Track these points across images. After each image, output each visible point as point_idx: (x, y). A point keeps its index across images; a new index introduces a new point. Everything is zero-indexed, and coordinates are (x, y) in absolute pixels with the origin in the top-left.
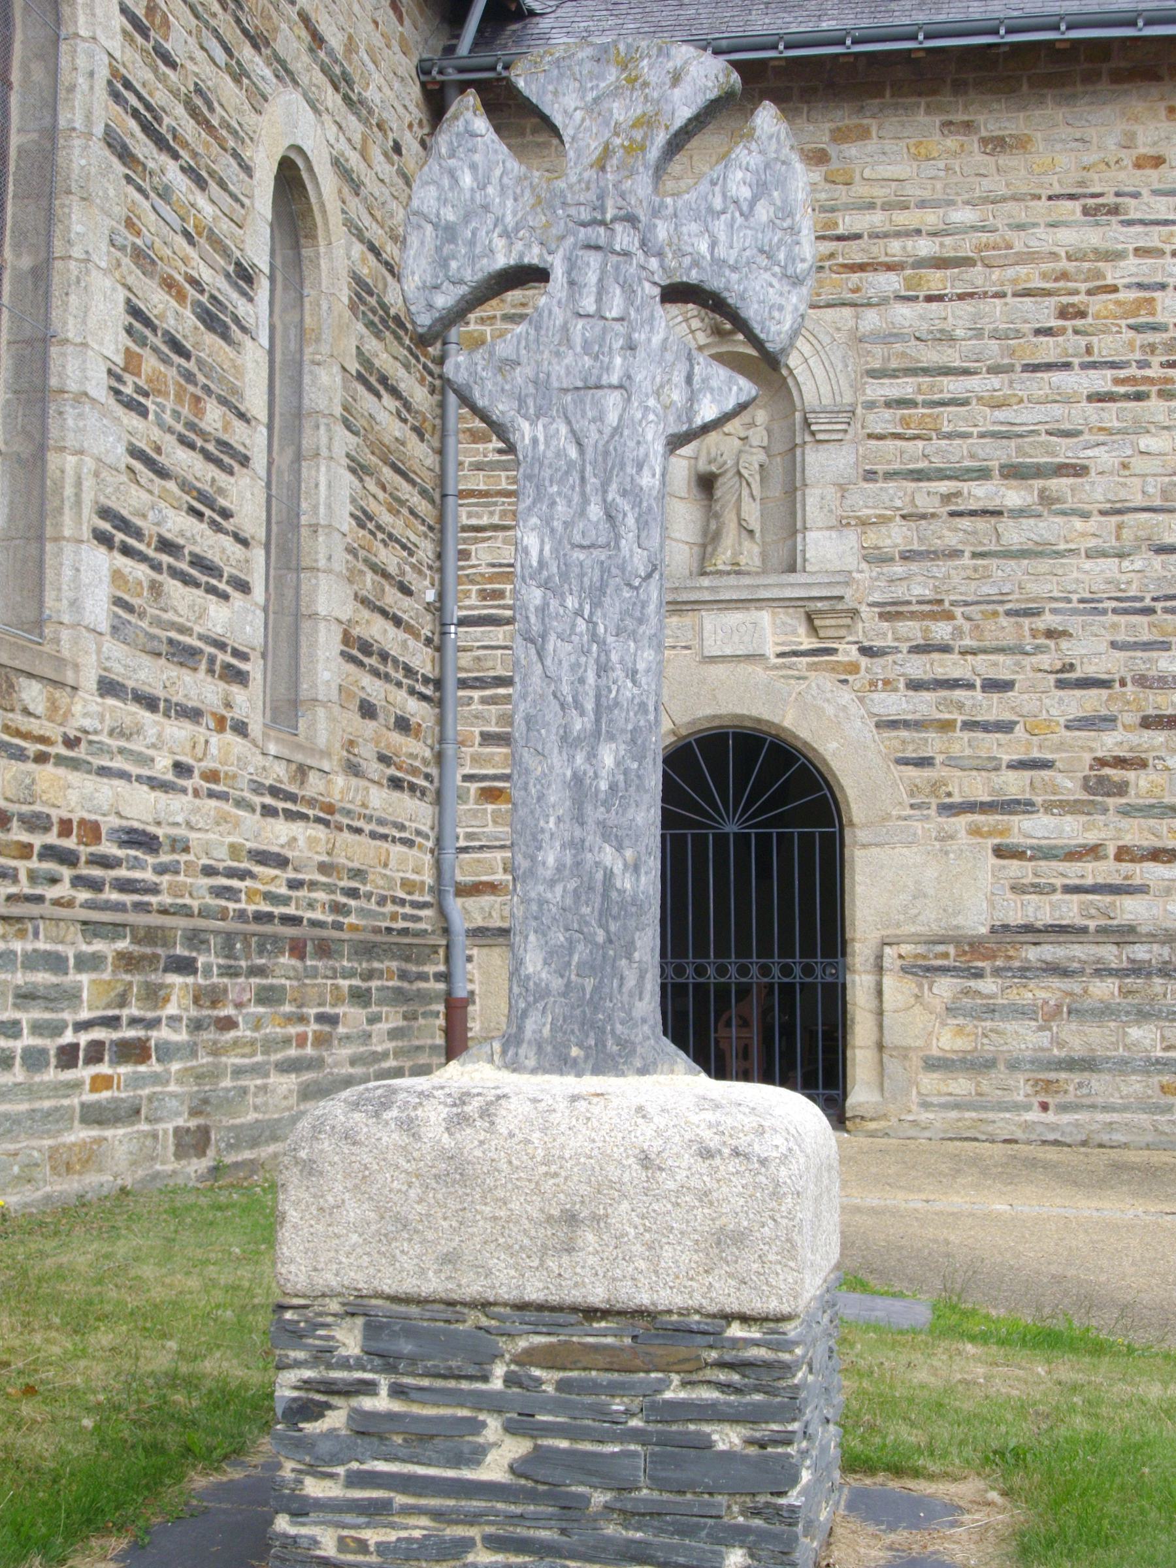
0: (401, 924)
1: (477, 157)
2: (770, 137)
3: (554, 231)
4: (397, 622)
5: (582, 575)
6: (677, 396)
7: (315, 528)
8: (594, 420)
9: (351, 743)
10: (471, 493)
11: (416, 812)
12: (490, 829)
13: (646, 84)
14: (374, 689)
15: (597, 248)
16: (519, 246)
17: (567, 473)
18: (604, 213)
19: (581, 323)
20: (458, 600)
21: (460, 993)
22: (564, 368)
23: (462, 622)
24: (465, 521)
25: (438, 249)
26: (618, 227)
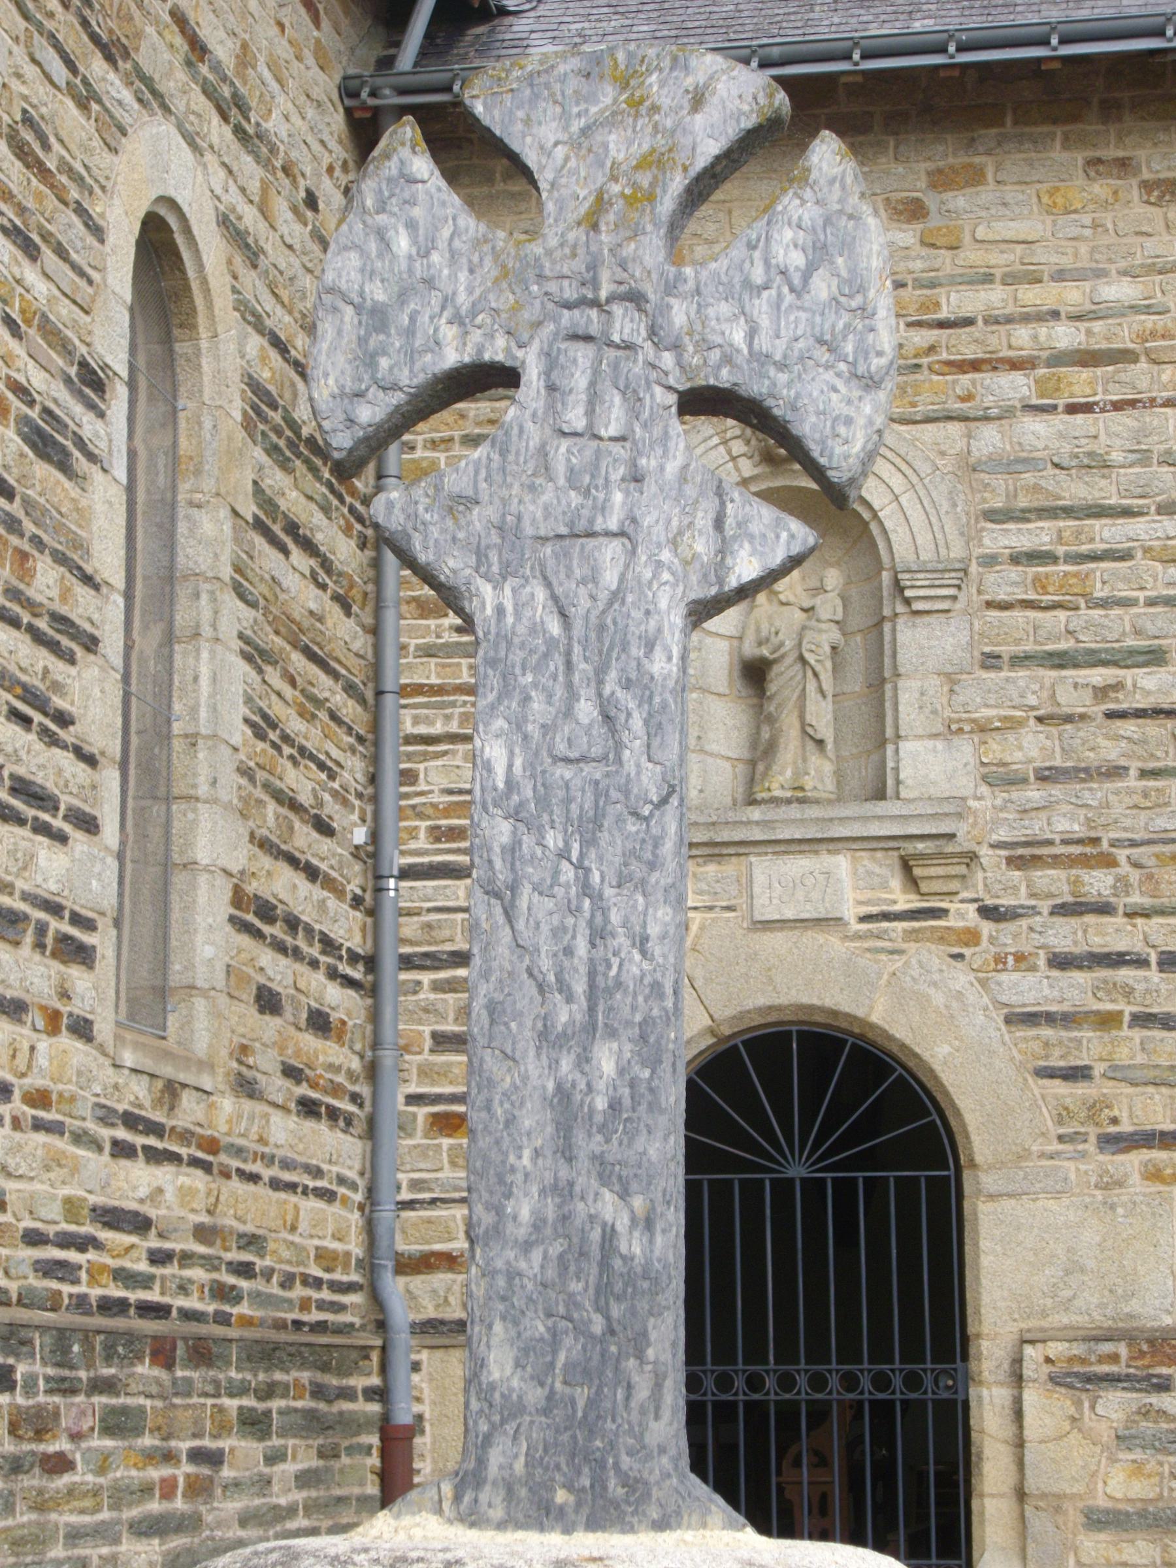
0: (315, 1316)
1: (417, 212)
2: (832, 182)
3: (526, 315)
4: (312, 873)
5: (568, 801)
6: (702, 546)
7: (192, 740)
8: (583, 582)
9: (244, 1049)
10: (418, 690)
11: (337, 1150)
12: (447, 1174)
13: (655, 109)
14: (278, 971)
15: (588, 338)
16: (476, 336)
17: (546, 656)
18: (596, 288)
19: (565, 444)
20: (399, 842)
21: (403, 1417)
22: (540, 509)
23: (406, 873)
24: (409, 728)
25: (362, 341)
26: (617, 309)
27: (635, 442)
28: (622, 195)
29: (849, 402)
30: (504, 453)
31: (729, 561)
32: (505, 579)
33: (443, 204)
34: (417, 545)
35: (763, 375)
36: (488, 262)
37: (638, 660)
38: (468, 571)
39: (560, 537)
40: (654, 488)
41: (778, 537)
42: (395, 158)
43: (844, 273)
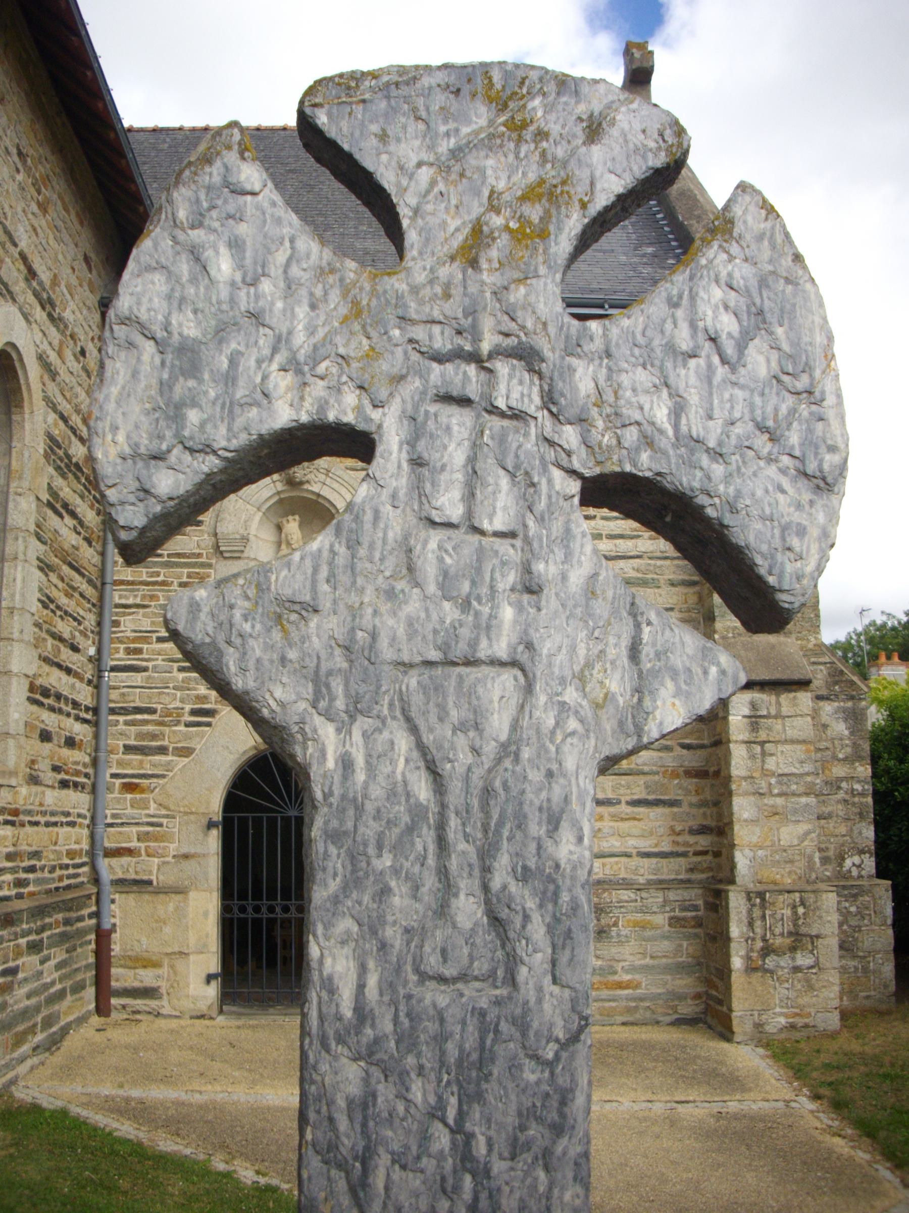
0: (66, 882)
1: (243, 229)
2: (760, 238)
3: (385, 366)
4: (68, 671)
5: (441, 1038)
6: (617, 684)
7: (12, 610)
8: (461, 728)
9: (33, 762)
10: (122, 582)
11: (78, 801)
12: (129, 811)
13: (542, 135)
14: (50, 720)
15: (464, 402)
16: (318, 389)
17: (411, 829)
18: (477, 339)
19: (435, 538)
20: (111, 654)
21: (106, 926)
22: (404, 623)
23: (114, 669)
24: (117, 600)
25: (165, 387)
26: (502, 367)
27: (527, 541)
28: (507, 228)
29: (799, 506)
30: (353, 545)
31: (647, 703)
32: (353, 718)
33: (279, 221)
34: (231, 664)
35: (695, 466)
36: (335, 296)
37: (539, 841)
38: (302, 705)
39: (428, 664)
40: (554, 604)
41: (706, 672)
42: (218, 165)
43: (786, 347)
